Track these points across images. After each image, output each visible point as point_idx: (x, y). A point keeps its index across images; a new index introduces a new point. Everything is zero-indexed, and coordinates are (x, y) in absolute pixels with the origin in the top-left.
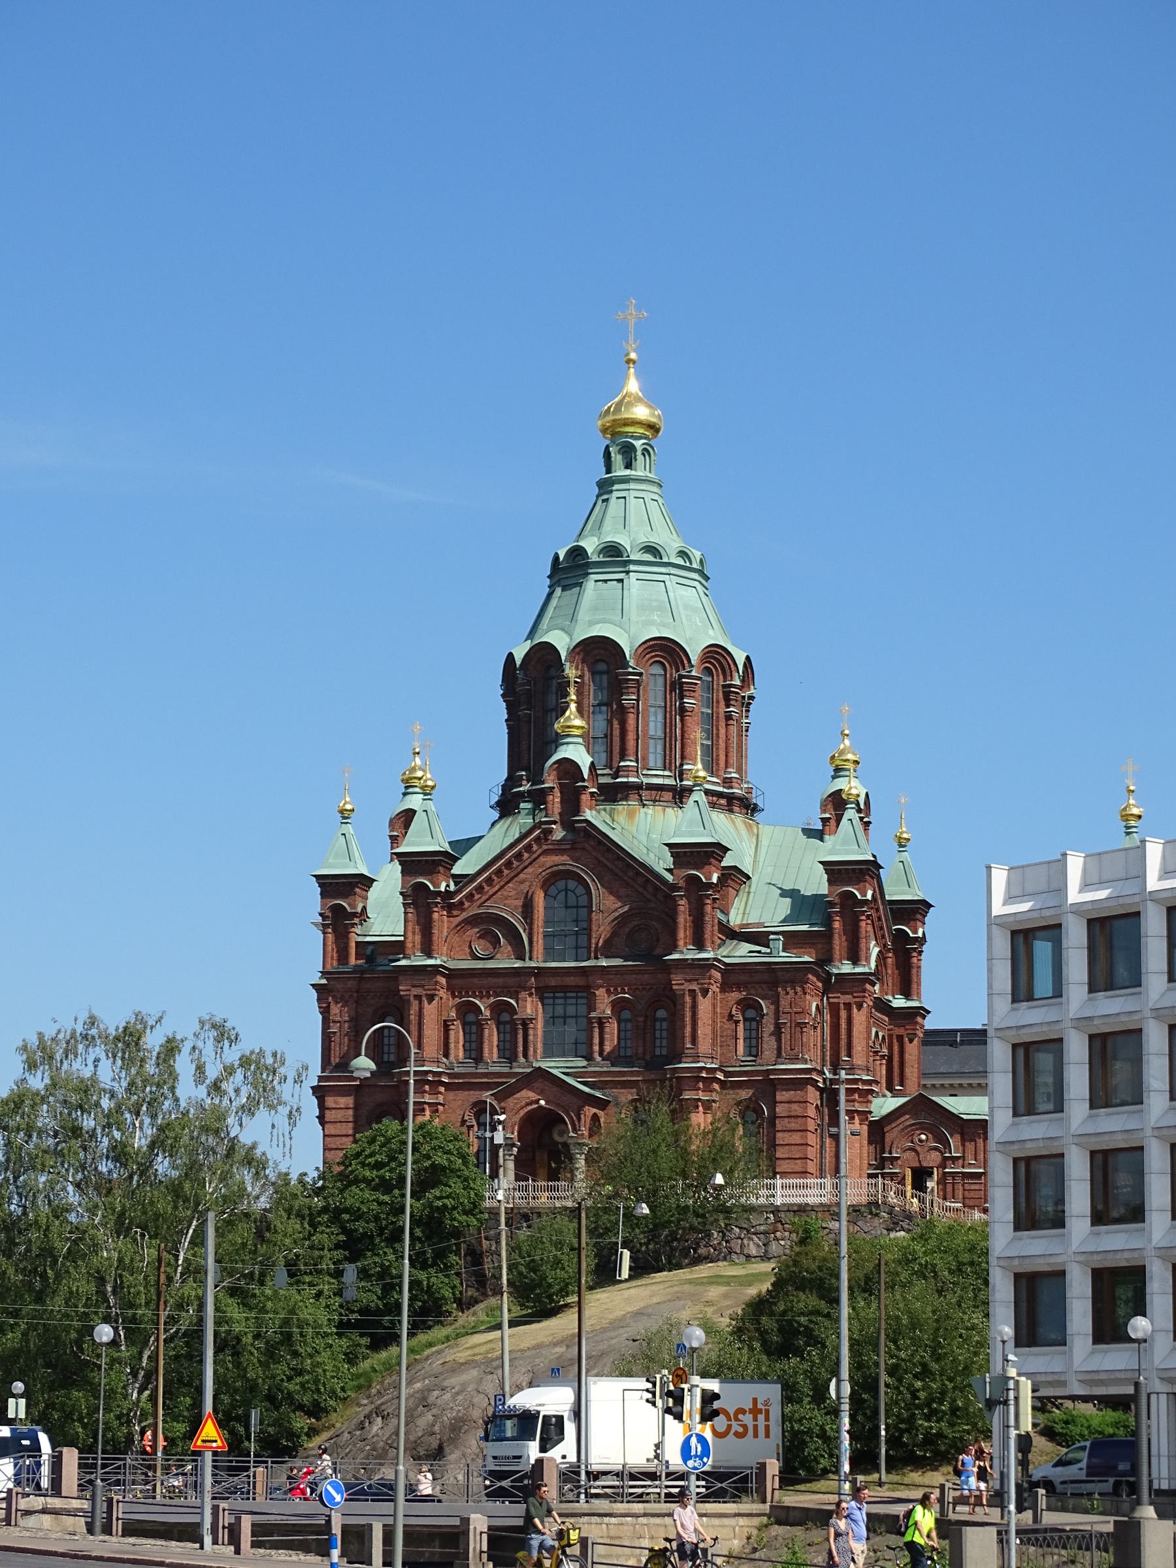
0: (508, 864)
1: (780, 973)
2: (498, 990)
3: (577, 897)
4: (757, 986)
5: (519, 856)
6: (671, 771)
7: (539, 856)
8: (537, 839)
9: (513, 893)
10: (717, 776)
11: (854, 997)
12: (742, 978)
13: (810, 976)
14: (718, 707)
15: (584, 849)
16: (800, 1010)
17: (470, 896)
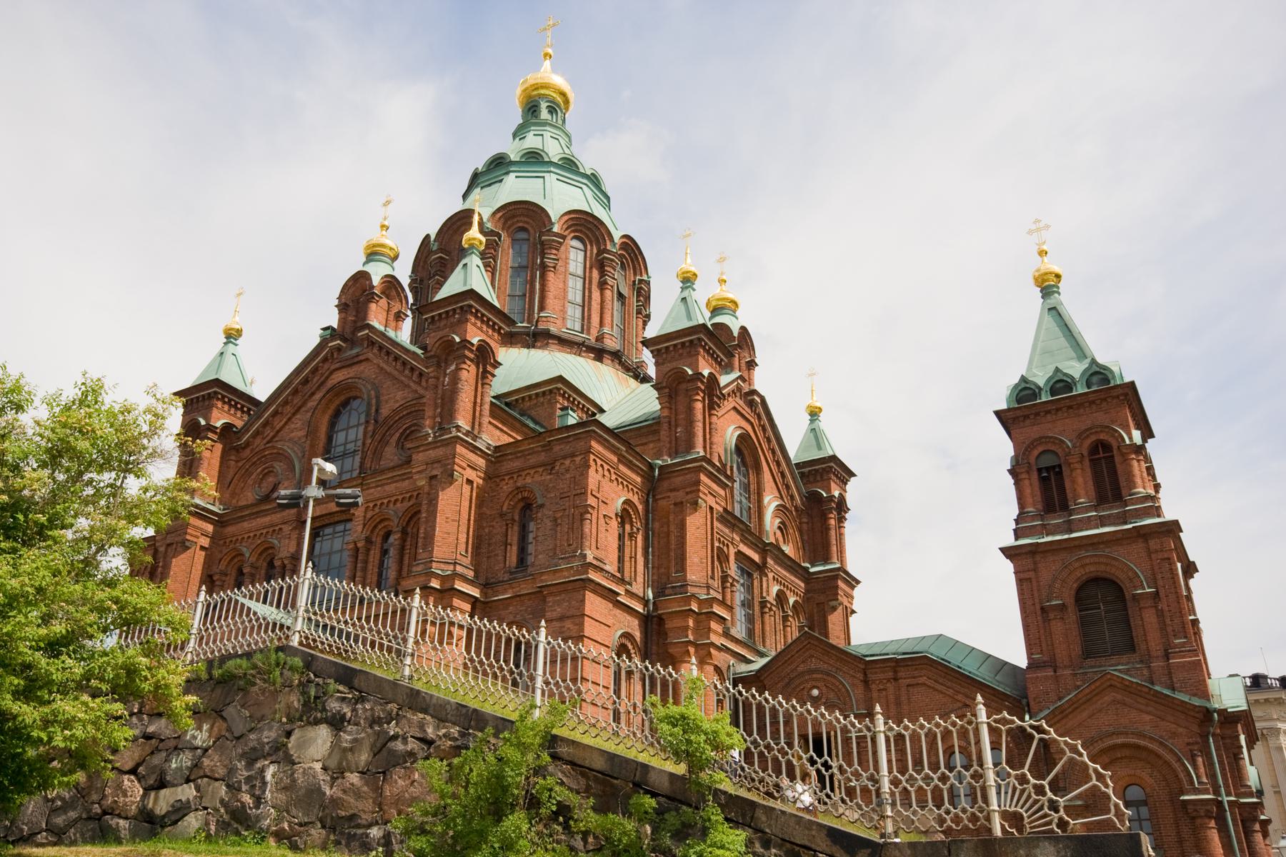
0: (295, 392)
1: (557, 448)
2: (264, 531)
3: (359, 414)
4: (532, 472)
5: (306, 381)
6: (528, 323)
7: (327, 378)
8: (325, 360)
9: (300, 423)
10: (589, 333)
11: (687, 493)
12: (515, 465)
13: (593, 443)
14: (591, 272)
15: (367, 360)
16: (579, 492)
17: (257, 433)
